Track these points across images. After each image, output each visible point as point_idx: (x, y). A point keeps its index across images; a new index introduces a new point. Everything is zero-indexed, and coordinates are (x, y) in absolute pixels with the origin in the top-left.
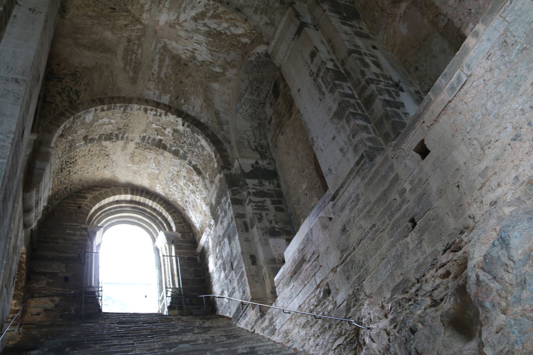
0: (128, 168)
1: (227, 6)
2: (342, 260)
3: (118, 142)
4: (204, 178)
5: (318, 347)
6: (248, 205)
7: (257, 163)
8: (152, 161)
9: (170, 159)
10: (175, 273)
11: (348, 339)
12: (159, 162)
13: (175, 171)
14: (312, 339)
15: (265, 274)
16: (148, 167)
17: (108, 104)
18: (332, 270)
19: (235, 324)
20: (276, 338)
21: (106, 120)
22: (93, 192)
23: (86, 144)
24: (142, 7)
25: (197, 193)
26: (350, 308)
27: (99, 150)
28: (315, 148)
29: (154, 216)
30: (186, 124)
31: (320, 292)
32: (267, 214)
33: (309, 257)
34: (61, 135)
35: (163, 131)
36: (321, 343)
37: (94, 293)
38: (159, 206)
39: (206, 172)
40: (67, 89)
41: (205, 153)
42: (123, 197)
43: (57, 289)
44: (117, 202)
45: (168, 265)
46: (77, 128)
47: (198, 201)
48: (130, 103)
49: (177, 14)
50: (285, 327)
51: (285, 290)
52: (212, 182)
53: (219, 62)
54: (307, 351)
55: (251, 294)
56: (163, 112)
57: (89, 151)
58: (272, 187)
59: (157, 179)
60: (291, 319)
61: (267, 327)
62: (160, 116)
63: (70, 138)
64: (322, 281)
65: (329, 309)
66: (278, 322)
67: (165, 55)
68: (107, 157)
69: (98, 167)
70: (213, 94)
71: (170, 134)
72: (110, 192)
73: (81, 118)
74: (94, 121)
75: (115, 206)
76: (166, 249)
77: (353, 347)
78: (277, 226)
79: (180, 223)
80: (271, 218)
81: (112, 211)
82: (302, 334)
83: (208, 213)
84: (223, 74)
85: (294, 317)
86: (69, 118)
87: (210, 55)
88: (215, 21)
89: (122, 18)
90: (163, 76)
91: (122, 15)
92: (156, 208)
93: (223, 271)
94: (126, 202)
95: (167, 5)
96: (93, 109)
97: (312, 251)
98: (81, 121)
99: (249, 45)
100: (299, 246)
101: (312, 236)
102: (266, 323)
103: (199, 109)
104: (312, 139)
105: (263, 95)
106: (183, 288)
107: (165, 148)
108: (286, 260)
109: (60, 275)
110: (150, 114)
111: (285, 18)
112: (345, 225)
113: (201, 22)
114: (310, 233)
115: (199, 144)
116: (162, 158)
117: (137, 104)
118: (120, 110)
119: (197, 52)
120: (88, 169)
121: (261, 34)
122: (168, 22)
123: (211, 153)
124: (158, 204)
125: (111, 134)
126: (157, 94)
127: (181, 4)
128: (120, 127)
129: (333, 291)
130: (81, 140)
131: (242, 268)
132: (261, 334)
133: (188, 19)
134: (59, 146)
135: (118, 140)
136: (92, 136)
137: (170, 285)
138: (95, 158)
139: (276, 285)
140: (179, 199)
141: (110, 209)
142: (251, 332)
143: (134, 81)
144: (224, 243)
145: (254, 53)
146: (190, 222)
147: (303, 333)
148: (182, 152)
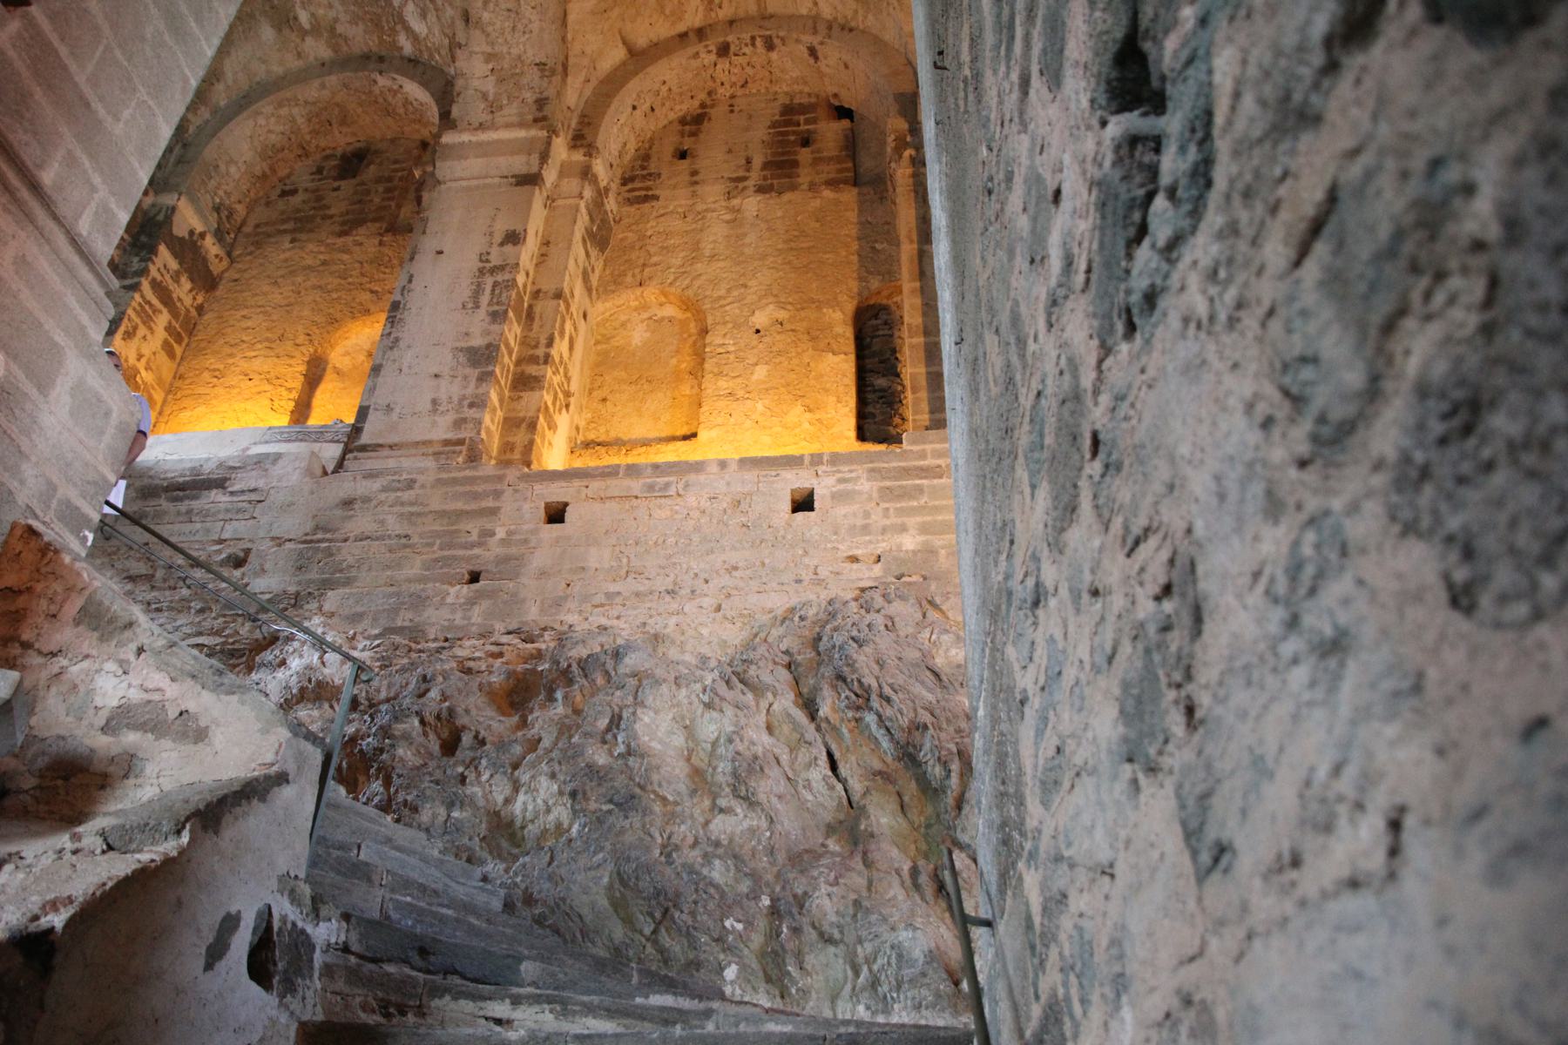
7: (202, 235)
58: (188, 301)
80: (146, 350)
99: (402, 58)
105: (323, 144)
111: (521, 134)
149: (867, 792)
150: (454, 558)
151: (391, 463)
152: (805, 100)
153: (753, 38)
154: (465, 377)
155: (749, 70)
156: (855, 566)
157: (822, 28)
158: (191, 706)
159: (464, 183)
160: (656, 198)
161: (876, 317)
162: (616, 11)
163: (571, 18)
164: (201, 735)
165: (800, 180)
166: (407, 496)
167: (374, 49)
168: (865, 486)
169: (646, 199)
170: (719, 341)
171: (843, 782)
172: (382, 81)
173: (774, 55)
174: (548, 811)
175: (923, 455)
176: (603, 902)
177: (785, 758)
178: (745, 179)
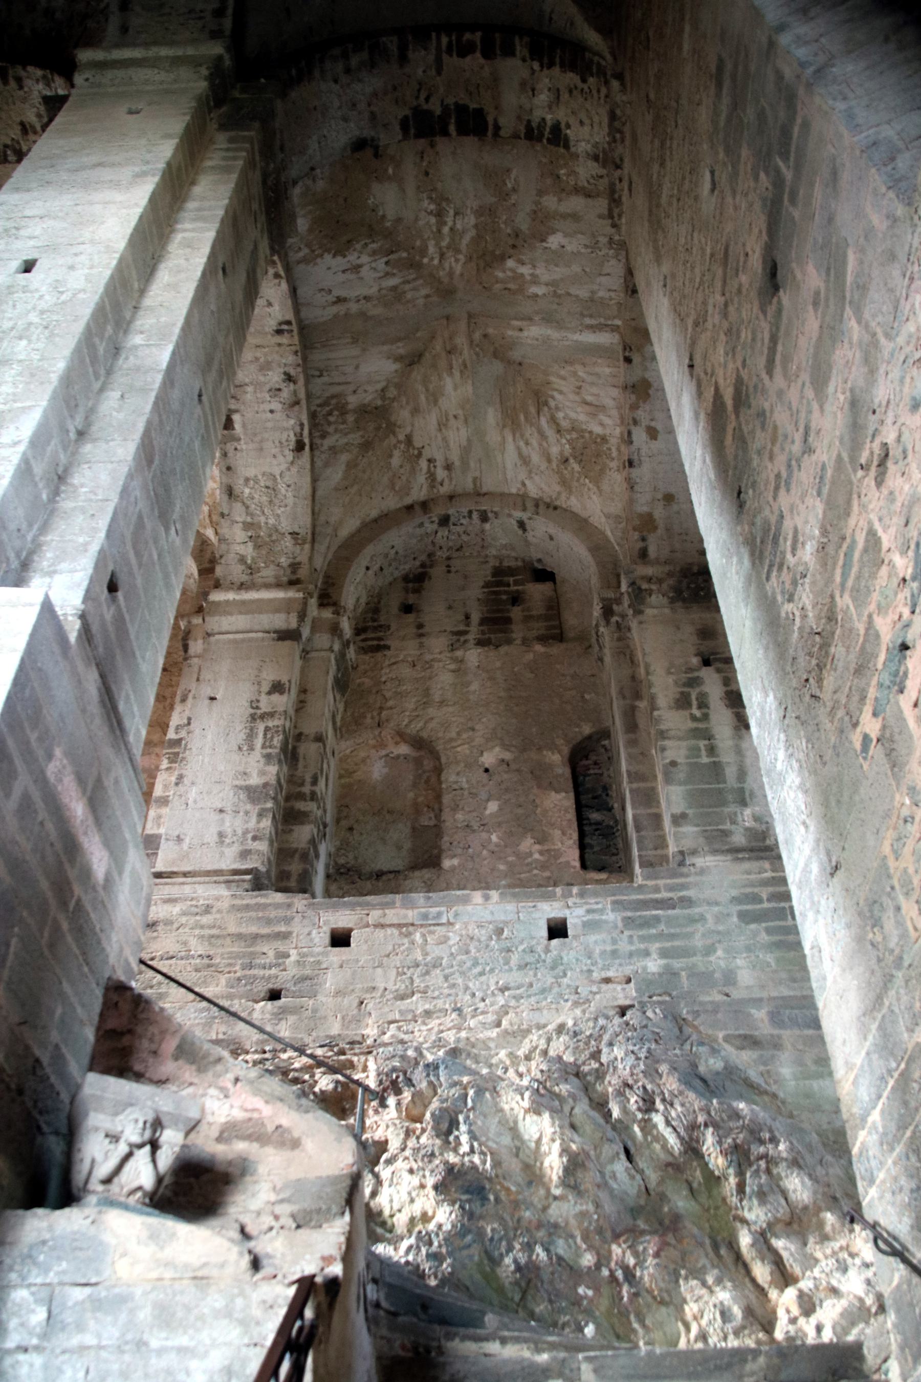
111: (280, 594)
149: (661, 1182)
150: (255, 977)
151: (187, 889)
152: (513, 564)
153: (470, 512)
154: (247, 813)
155: (465, 538)
156: (610, 986)
157: (530, 505)
158: (285, 1122)
159: (231, 636)
160: (388, 648)
161: (587, 758)
162: (356, 488)
163: (319, 493)
164: (295, 1144)
165: (514, 635)
166: (205, 920)
168: (611, 916)
169: (378, 648)
170: (453, 778)
171: (641, 1172)
173: (487, 526)
174: (412, 1201)
175: (657, 890)
176: (478, 1277)
177: (592, 1153)
178: (465, 633)
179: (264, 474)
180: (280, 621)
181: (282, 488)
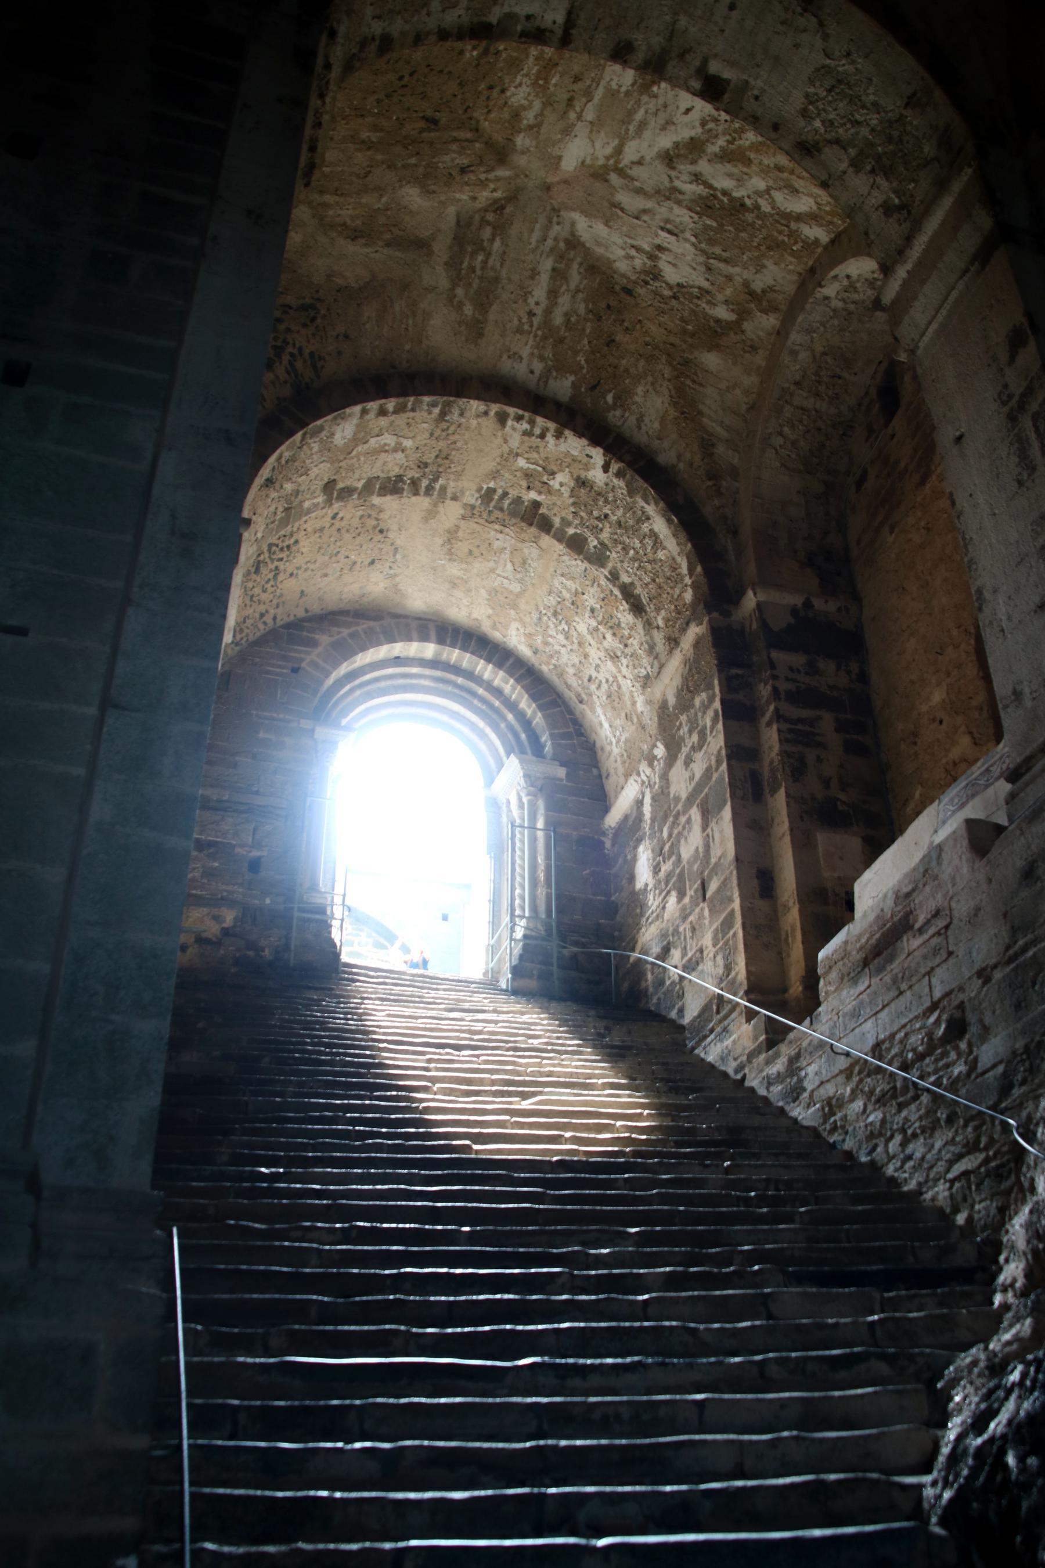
0: (434, 569)
1: (773, 135)
2: (1011, 952)
3: (414, 499)
4: (649, 625)
5: (911, 1163)
6: (769, 724)
8: (506, 555)
9: (556, 555)
10: (542, 876)
11: (993, 1164)
12: (524, 562)
13: (568, 590)
14: (898, 1138)
15: (793, 930)
16: (493, 571)
17: (398, 395)
18: (980, 974)
19: (693, 1049)
20: (803, 1114)
21: (389, 439)
22: (335, 629)
23: (329, 502)
24: (516, 115)
25: (624, 661)
26: (1011, 1086)
27: (361, 517)
28: (983, 618)
29: (492, 706)
30: (615, 467)
31: (938, 1022)
32: (819, 760)
33: (921, 919)
34: (267, 480)
35: (545, 479)
36: (918, 1155)
37: (322, 910)
38: (512, 681)
39: (658, 610)
40: (290, 349)
41: (661, 555)
42: (413, 649)
43: (230, 888)
44: (398, 661)
45: (523, 851)
46: (307, 461)
47: (626, 685)
48: (459, 395)
49: (616, 142)
50: (830, 1090)
51: (845, 992)
52: (673, 642)
53: (729, 291)
54: (879, 1164)
55: (748, 978)
56: (552, 426)
57: (334, 518)
59: (515, 606)
60: (848, 1073)
61: (779, 1078)
62: (542, 436)
63: (289, 487)
64: (947, 994)
65: (956, 1072)
66: (812, 1071)
67: (572, 260)
68: (380, 537)
69: (355, 563)
70: (701, 385)
71: (566, 491)
72: (378, 630)
73: (323, 434)
74: (358, 439)
75: (390, 671)
76: (521, 806)
77: (1002, 1187)
78: (842, 796)
79: (566, 736)
81: (383, 684)
82: (871, 1119)
83: (651, 721)
84: (736, 326)
85: (857, 1069)
86: (292, 433)
87: (703, 269)
88: (729, 167)
89: (454, 147)
90: (558, 320)
91: (456, 140)
92: (503, 685)
93: (674, 894)
94: (422, 662)
95: (590, 115)
96: (357, 409)
97: (932, 905)
98: (321, 441)
99: (826, 248)
100: (900, 882)
101: (939, 864)
102: (779, 1066)
103: (657, 425)
104: (979, 592)
106: (559, 923)
107: (545, 525)
108: (858, 912)
109: (238, 850)
110: (514, 429)
111: (947, 202)
112: (1034, 861)
113: (685, 168)
114: (934, 855)
115: (645, 527)
116: (535, 552)
117: (478, 398)
118: (430, 413)
119: (664, 257)
120: (327, 566)
121: (866, 233)
122: (588, 161)
123: (679, 559)
124: (511, 675)
125: (400, 478)
126: (537, 373)
127: (630, 113)
128: (425, 459)
129: (974, 1030)
130: (318, 492)
131: (731, 900)
132: (762, 1092)
133: (648, 158)
134: (259, 511)
135: (416, 493)
136: (348, 483)
137: (523, 909)
138: (347, 536)
139: (820, 971)
140: (571, 671)
141: (376, 680)
142: (735, 1081)
143: (476, 330)
144: (689, 821)
145: (836, 277)
146: (593, 737)
147: (875, 1117)
148: (593, 542)
167: (800, 269)
172: (830, 290)
179: (811, 82)
180: (969, 240)
181: (844, 67)
